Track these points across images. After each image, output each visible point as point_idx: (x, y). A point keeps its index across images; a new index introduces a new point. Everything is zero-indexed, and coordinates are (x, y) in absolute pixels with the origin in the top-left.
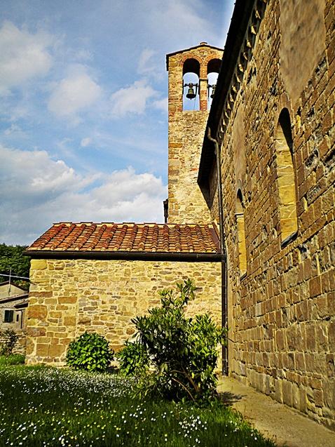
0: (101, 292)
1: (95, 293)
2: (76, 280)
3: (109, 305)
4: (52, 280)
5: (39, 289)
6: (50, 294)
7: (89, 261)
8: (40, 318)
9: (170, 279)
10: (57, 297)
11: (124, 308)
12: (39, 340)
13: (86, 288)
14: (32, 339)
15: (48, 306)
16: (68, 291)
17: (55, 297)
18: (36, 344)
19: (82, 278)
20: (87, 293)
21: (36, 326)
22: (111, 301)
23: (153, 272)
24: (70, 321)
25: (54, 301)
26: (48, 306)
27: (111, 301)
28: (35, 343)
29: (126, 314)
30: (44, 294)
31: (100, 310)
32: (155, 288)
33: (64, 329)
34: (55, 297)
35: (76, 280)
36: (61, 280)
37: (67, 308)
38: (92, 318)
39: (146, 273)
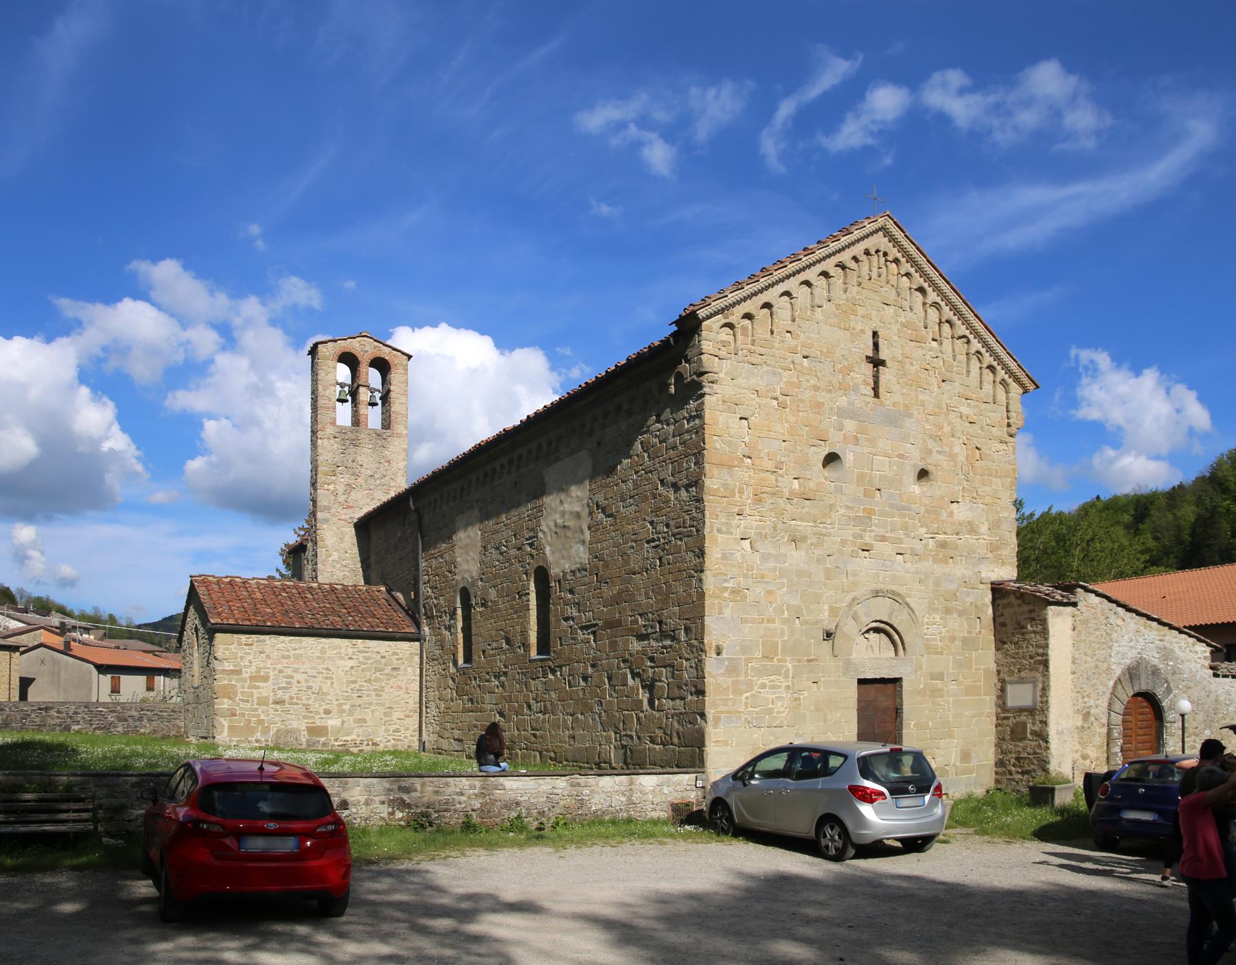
0: (296, 671)
1: (289, 672)
2: (268, 657)
3: (304, 685)
4: (242, 658)
5: (228, 666)
6: (239, 672)
7: (282, 638)
8: (230, 698)
9: (368, 658)
10: (247, 676)
11: (321, 688)
12: (231, 721)
13: (279, 667)
14: (222, 720)
15: (239, 685)
16: (259, 669)
17: (244, 675)
18: (226, 724)
19: (275, 655)
20: (281, 671)
21: (225, 706)
22: (307, 681)
23: (350, 650)
24: (263, 702)
25: (244, 680)
26: (239, 685)
27: (307, 681)
28: (226, 724)
29: (324, 694)
30: (232, 672)
31: (294, 690)
32: (352, 667)
33: (256, 710)
34: (244, 675)
35: (268, 657)
36: (251, 657)
37: (258, 687)
38: (286, 698)
39: (343, 651)
